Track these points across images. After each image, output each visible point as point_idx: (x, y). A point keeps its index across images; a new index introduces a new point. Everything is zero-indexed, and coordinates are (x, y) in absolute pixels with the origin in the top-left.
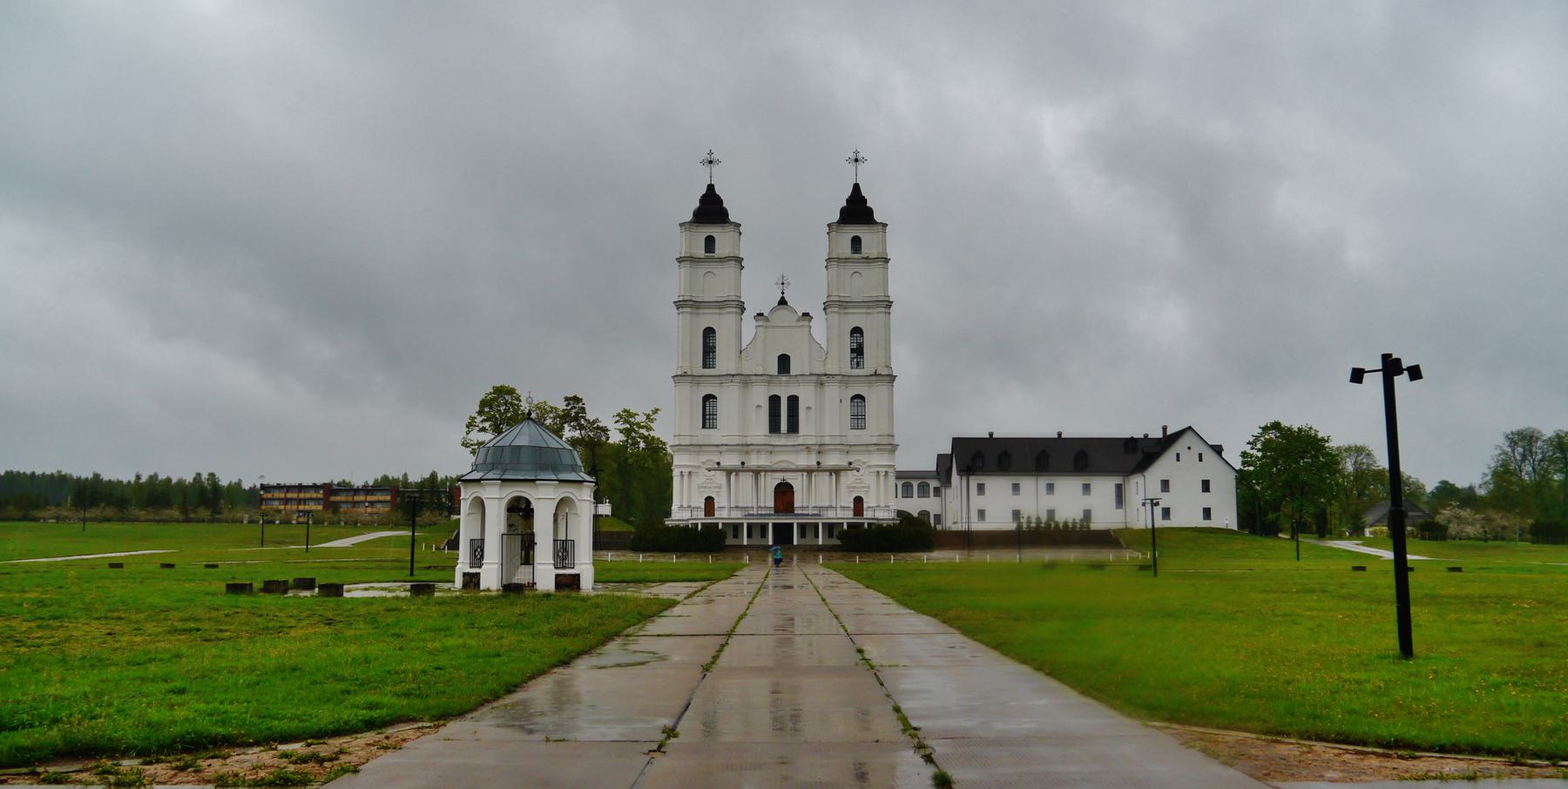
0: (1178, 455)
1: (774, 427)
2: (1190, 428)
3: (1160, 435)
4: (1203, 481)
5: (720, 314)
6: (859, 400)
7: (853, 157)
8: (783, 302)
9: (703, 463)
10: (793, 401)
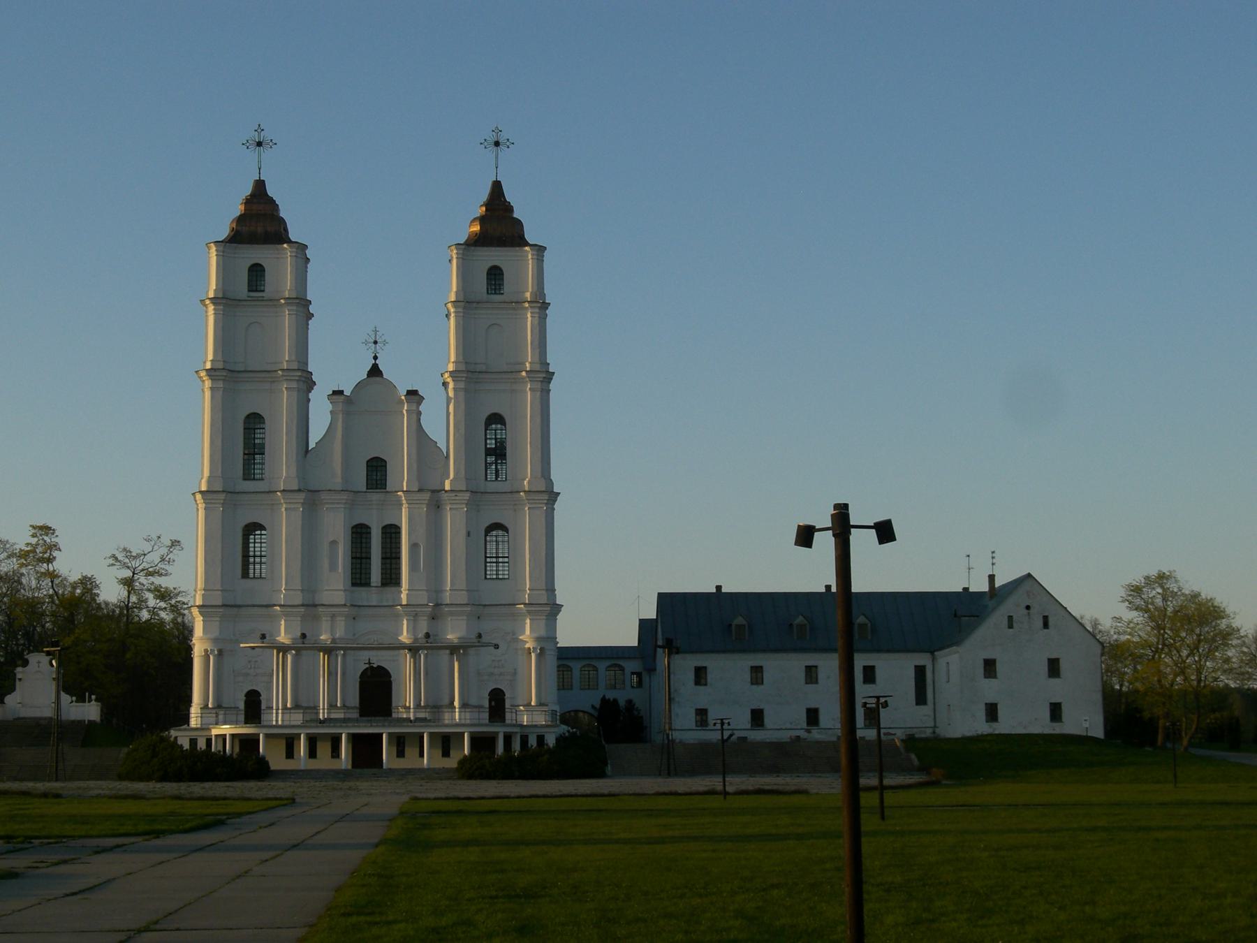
0: (1010, 618)
1: (359, 578)
2: (1029, 575)
3: (984, 587)
6: (500, 533)
7: (492, 138)
8: (375, 371)
10: (391, 533)
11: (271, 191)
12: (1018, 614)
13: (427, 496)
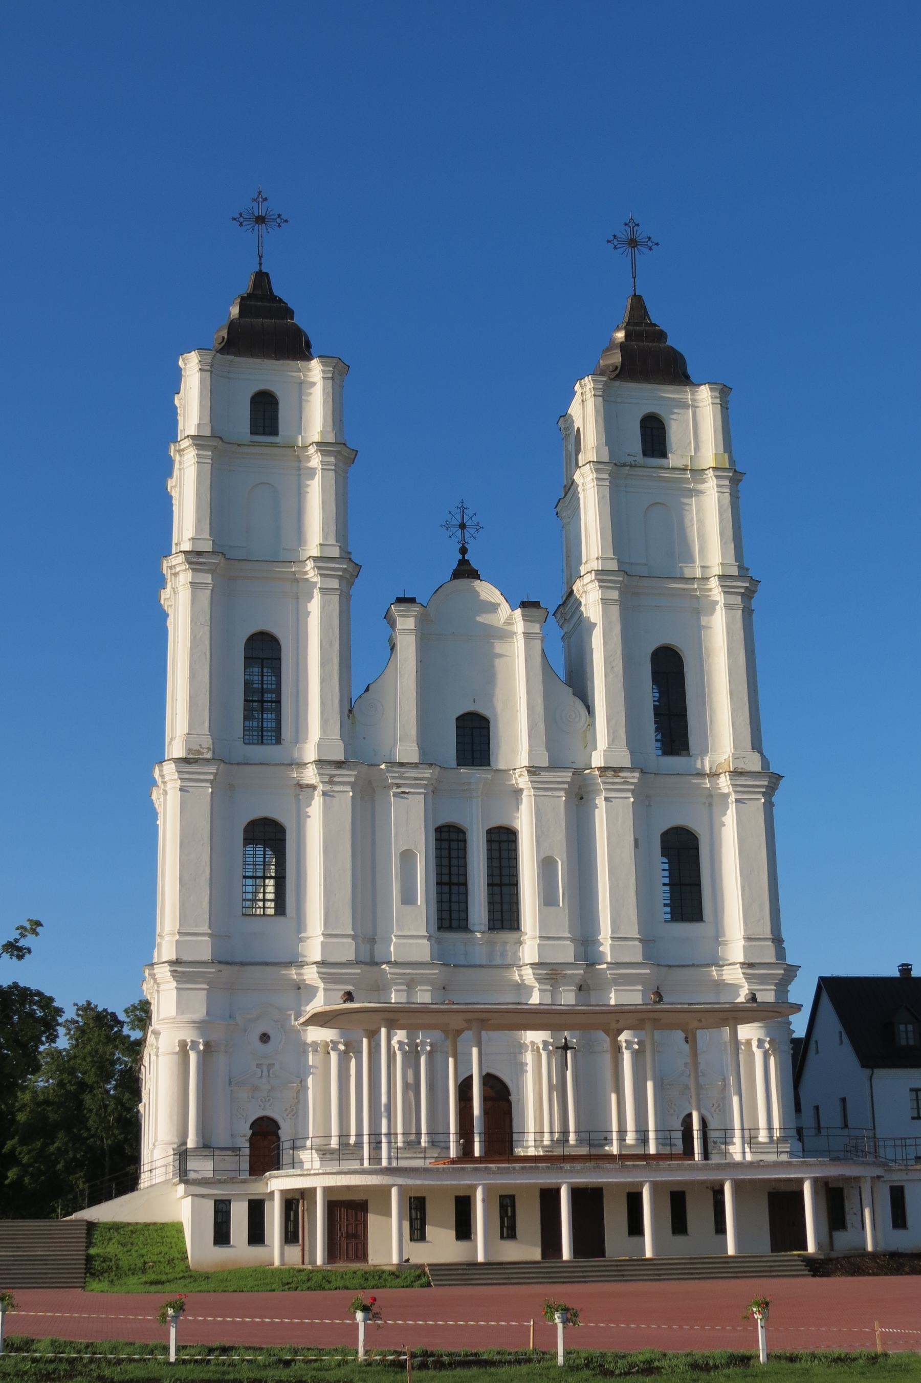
7: (624, 234)
11: (278, 290)
13: (567, 776)
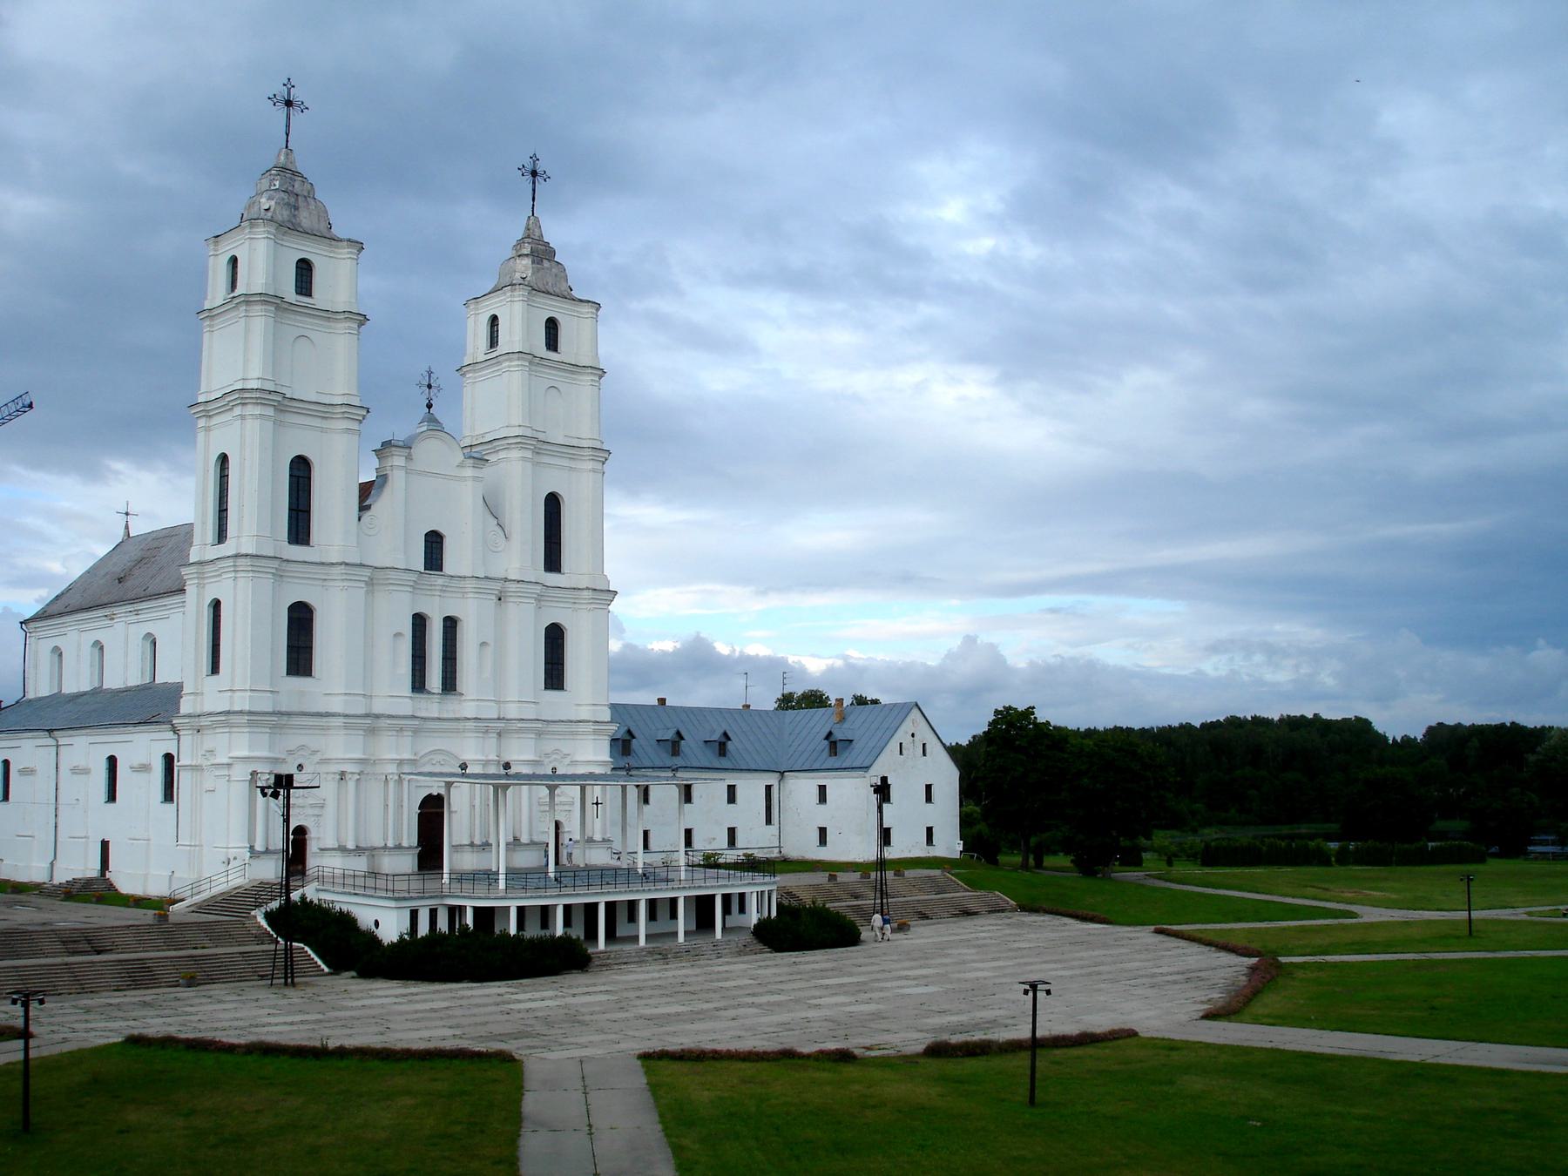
4: (927, 785)
5: (323, 430)
7: (529, 167)
9: (290, 752)
12: (907, 740)
